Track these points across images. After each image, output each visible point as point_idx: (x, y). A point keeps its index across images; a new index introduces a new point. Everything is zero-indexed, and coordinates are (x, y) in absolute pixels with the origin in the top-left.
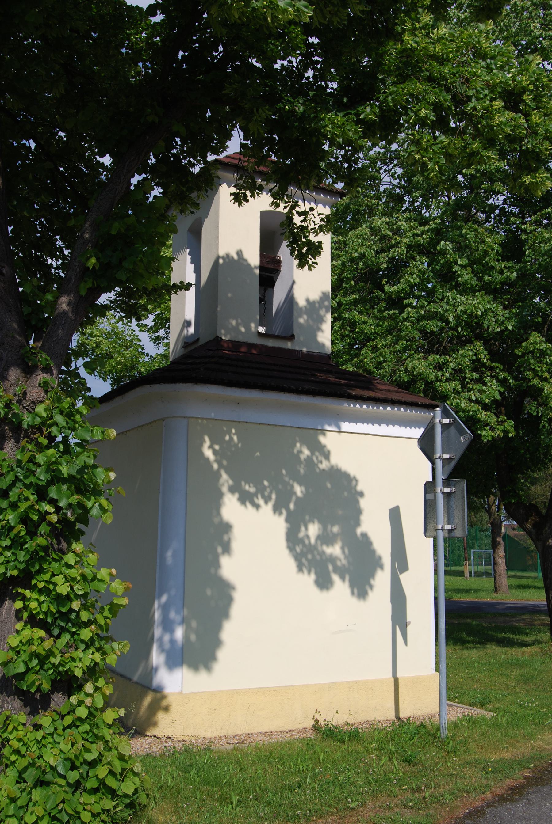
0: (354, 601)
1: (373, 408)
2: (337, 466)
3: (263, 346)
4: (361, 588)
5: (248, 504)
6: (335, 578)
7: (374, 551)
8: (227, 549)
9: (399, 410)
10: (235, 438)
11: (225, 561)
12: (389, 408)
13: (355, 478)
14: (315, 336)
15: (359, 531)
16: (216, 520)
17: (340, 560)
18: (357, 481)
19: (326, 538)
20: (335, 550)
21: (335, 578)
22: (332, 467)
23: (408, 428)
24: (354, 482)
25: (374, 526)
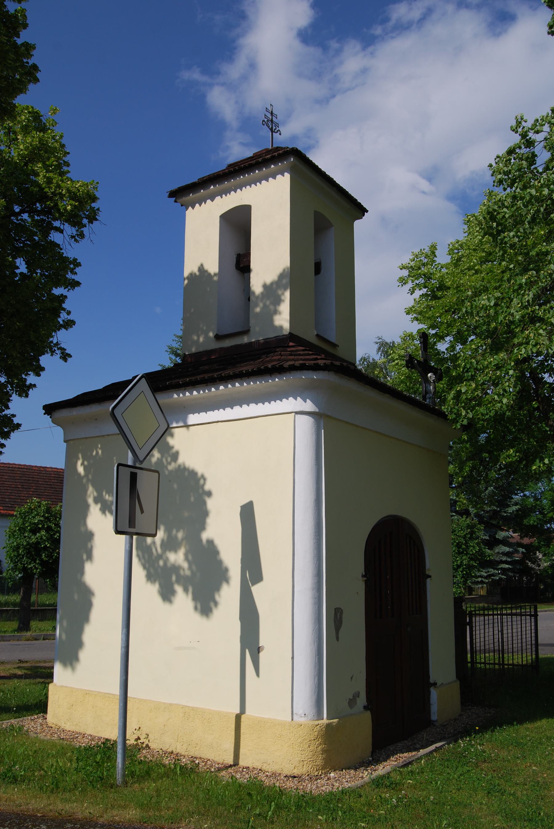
0: (197, 617)
1: (204, 391)
2: (184, 464)
3: (221, 349)
4: (205, 604)
5: (107, 513)
6: (179, 589)
7: (220, 562)
8: (90, 557)
9: (234, 385)
10: (100, 452)
11: (88, 567)
12: (222, 387)
13: (203, 476)
14: (272, 321)
15: (205, 536)
16: (83, 529)
17: (184, 570)
18: (205, 480)
19: (170, 545)
20: (177, 558)
21: (179, 589)
22: (179, 466)
23: (267, 403)
24: (202, 482)
25: (222, 531)
